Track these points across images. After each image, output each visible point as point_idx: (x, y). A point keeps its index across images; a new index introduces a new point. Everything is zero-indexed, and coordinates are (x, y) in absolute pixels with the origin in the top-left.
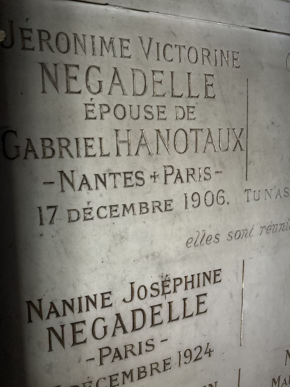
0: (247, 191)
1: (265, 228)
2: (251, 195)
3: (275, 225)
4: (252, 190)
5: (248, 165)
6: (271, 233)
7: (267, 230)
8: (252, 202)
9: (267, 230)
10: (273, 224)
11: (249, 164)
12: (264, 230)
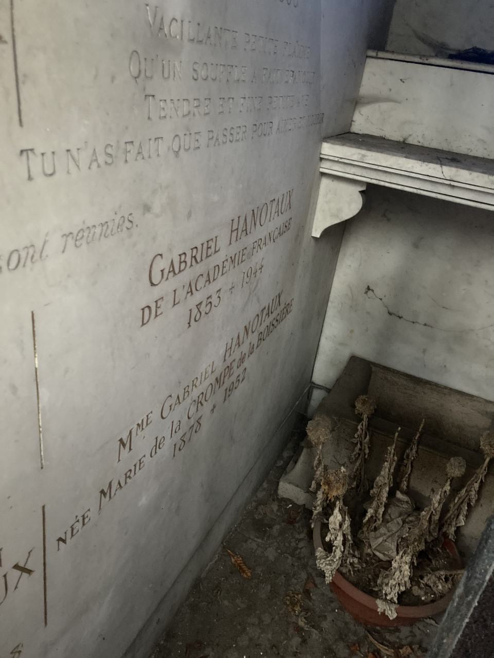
0: (25, 154)
1: (71, 236)
2: (36, 163)
3: (91, 227)
4: (39, 151)
5: (21, 85)
6: (84, 246)
7: (76, 240)
8: (40, 180)
9: (76, 240)
10: (86, 227)
11: (24, 83)
12: (71, 241)
